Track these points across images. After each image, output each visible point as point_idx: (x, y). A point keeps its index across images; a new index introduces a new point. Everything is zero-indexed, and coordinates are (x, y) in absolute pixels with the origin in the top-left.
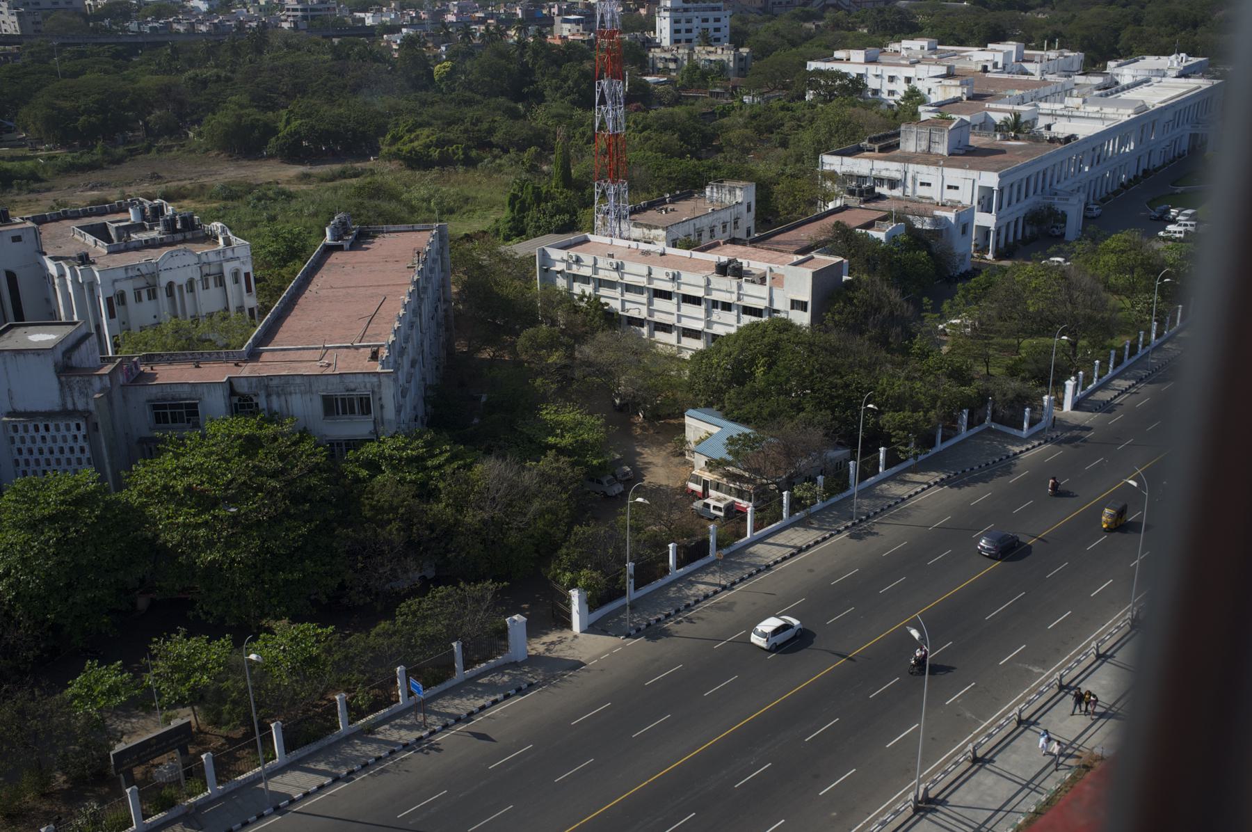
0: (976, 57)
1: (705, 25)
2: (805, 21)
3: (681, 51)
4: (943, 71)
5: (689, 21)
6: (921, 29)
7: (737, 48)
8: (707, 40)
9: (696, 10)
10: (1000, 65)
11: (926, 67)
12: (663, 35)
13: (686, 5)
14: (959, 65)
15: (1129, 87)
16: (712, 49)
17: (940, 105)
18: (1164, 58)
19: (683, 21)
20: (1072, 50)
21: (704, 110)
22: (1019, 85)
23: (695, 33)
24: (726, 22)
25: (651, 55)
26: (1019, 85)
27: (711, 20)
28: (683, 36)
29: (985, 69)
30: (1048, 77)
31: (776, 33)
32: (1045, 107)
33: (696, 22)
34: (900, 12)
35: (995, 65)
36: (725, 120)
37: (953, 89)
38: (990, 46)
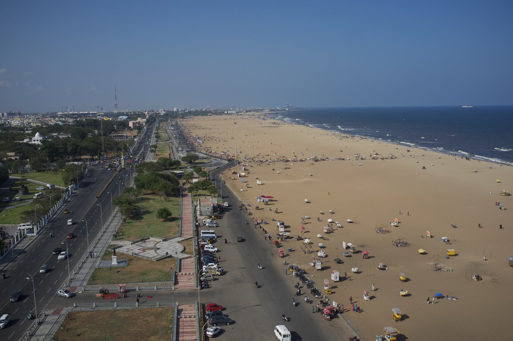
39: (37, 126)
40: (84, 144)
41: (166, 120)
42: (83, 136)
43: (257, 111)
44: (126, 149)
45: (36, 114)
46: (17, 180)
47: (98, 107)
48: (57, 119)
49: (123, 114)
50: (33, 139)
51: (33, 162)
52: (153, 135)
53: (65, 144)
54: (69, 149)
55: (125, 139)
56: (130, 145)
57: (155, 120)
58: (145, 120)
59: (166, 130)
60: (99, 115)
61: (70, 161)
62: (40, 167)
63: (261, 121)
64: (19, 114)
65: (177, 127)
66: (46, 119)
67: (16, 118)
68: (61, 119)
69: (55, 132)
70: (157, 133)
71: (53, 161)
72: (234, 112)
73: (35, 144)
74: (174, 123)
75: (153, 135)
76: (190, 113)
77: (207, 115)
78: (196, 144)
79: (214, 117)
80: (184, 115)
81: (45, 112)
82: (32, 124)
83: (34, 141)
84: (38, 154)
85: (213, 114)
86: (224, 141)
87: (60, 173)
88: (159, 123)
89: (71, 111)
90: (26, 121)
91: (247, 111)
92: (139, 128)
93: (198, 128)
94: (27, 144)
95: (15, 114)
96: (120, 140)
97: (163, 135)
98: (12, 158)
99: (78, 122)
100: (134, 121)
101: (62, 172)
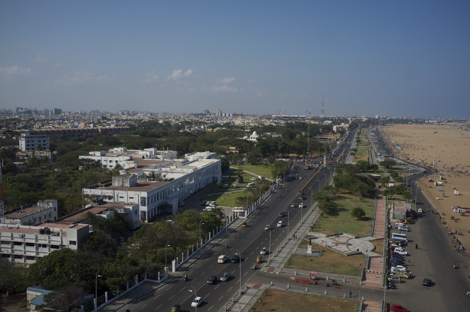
0: (141, 153)
1: (40, 143)
2: (79, 142)
3: (29, 153)
4: (129, 158)
5: (33, 141)
6: (122, 144)
7: (52, 151)
8: (40, 148)
9: (36, 137)
10: (149, 156)
11: (122, 157)
12: (22, 147)
13: (31, 136)
14: (134, 156)
15: (192, 162)
16: (42, 152)
17: (127, 170)
18: (203, 153)
19: (30, 141)
20: (174, 151)
21: (39, 174)
22: (155, 162)
23: (36, 146)
24: (48, 142)
25: (17, 154)
26: (155, 162)
27: (42, 141)
28: (31, 147)
29: (143, 157)
30: (165, 159)
31: (68, 146)
32: (164, 169)
33: (36, 142)
34: (114, 138)
35: (147, 156)
36: (47, 178)
37: (132, 164)
38: (145, 149)
39: (255, 126)
40: (292, 143)
41: (368, 127)
42: (292, 136)
43: (460, 121)
44: (329, 151)
45: (254, 116)
46: (236, 170)
47: (307, 112)
48: (271, 120)
49: (328, 119)
50: (251, 136)
51: (249, 156)
52: (355, 140)
53: (276, 143)
54: (280, 147)
55: (329, 142)
56: (332, 147)
57: (357, 126)
58: (348, 125)
59: (366, 135)
60: (307, 119)
61: (279, 158)
62: (254, 161)
63: (463, 131)
64: (242, 115)
65: (377, 133)
66: (263, 120)
67: (239, 118)
68: (275, 121)
69: (269, 132)
70: (358, 138)
71: (265, 157)
72: (435, 122)
73: (252, 141)
74: (374, 129)
75: (355, 140)
76: (391, 120)
77: (408, 123)
78: (395, 151)
79: (414, 125)
80: (385, 122)
81: (262, 115)
82: (251, 124)
83: (252, 138)
85: (414, 122)
86: (423, 149)
87: (270, 167)
88: (361, 129)
89: (283, 114)
90: (246, 121)
91: (449, 122)
92: (342, 132)
93: (397, 135)
94: (245, 141)
95: (238, 115)
96: (324, 142)
97: (364, 140)
98: (234, 152)
99: (288, 124)
100: (338, 126)
101: (272, 166)
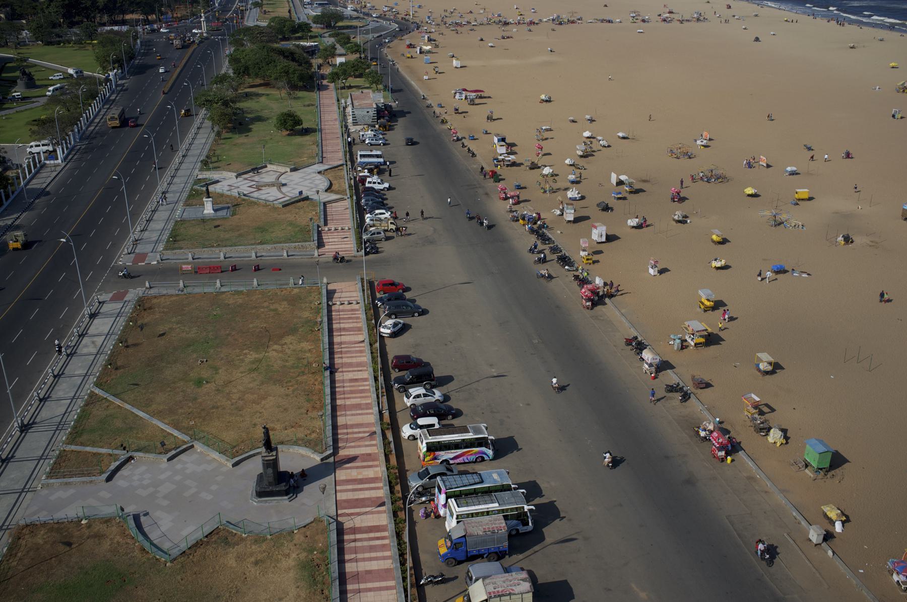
46: (10, 60)
61: (104, 25)
71: (72, 25)
84: (42, 9)
87: (90, 48)
101: (93, 45)
